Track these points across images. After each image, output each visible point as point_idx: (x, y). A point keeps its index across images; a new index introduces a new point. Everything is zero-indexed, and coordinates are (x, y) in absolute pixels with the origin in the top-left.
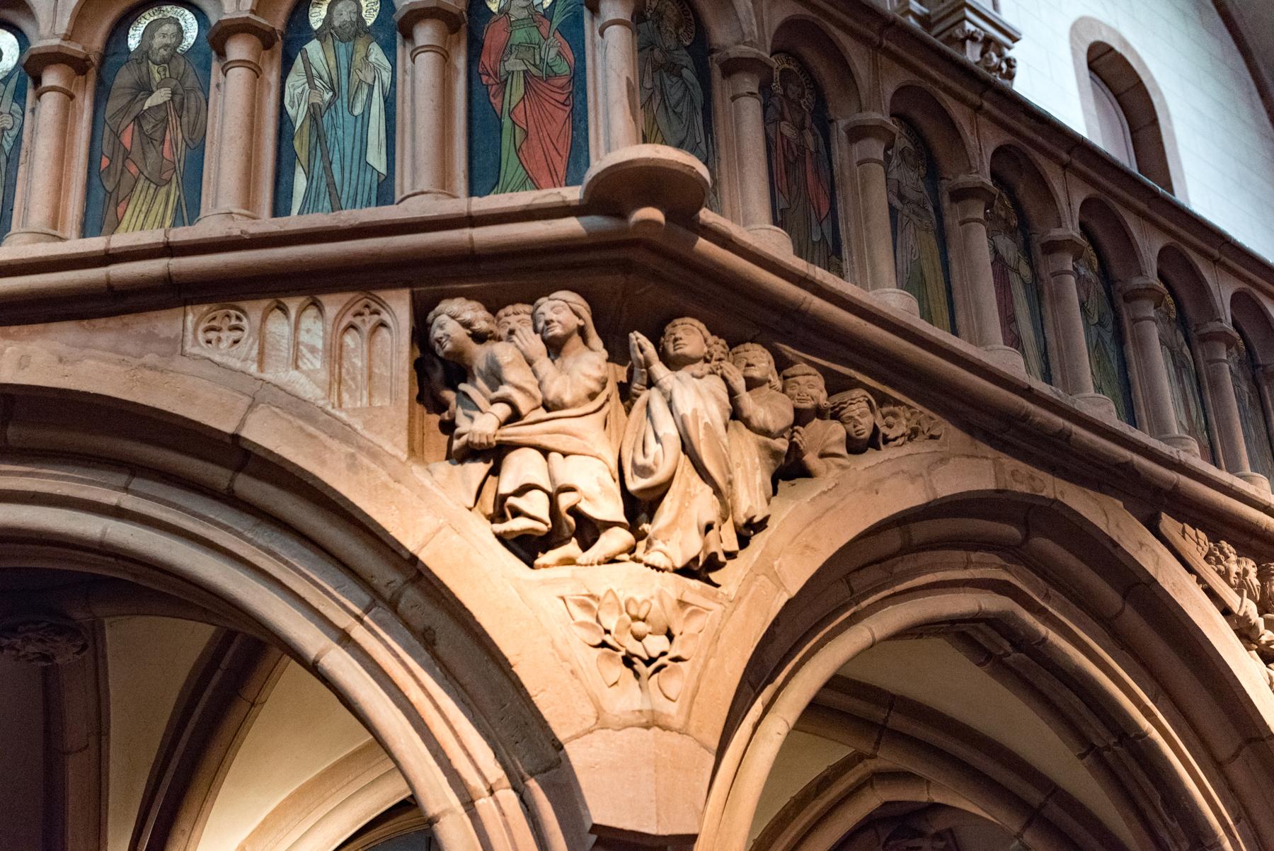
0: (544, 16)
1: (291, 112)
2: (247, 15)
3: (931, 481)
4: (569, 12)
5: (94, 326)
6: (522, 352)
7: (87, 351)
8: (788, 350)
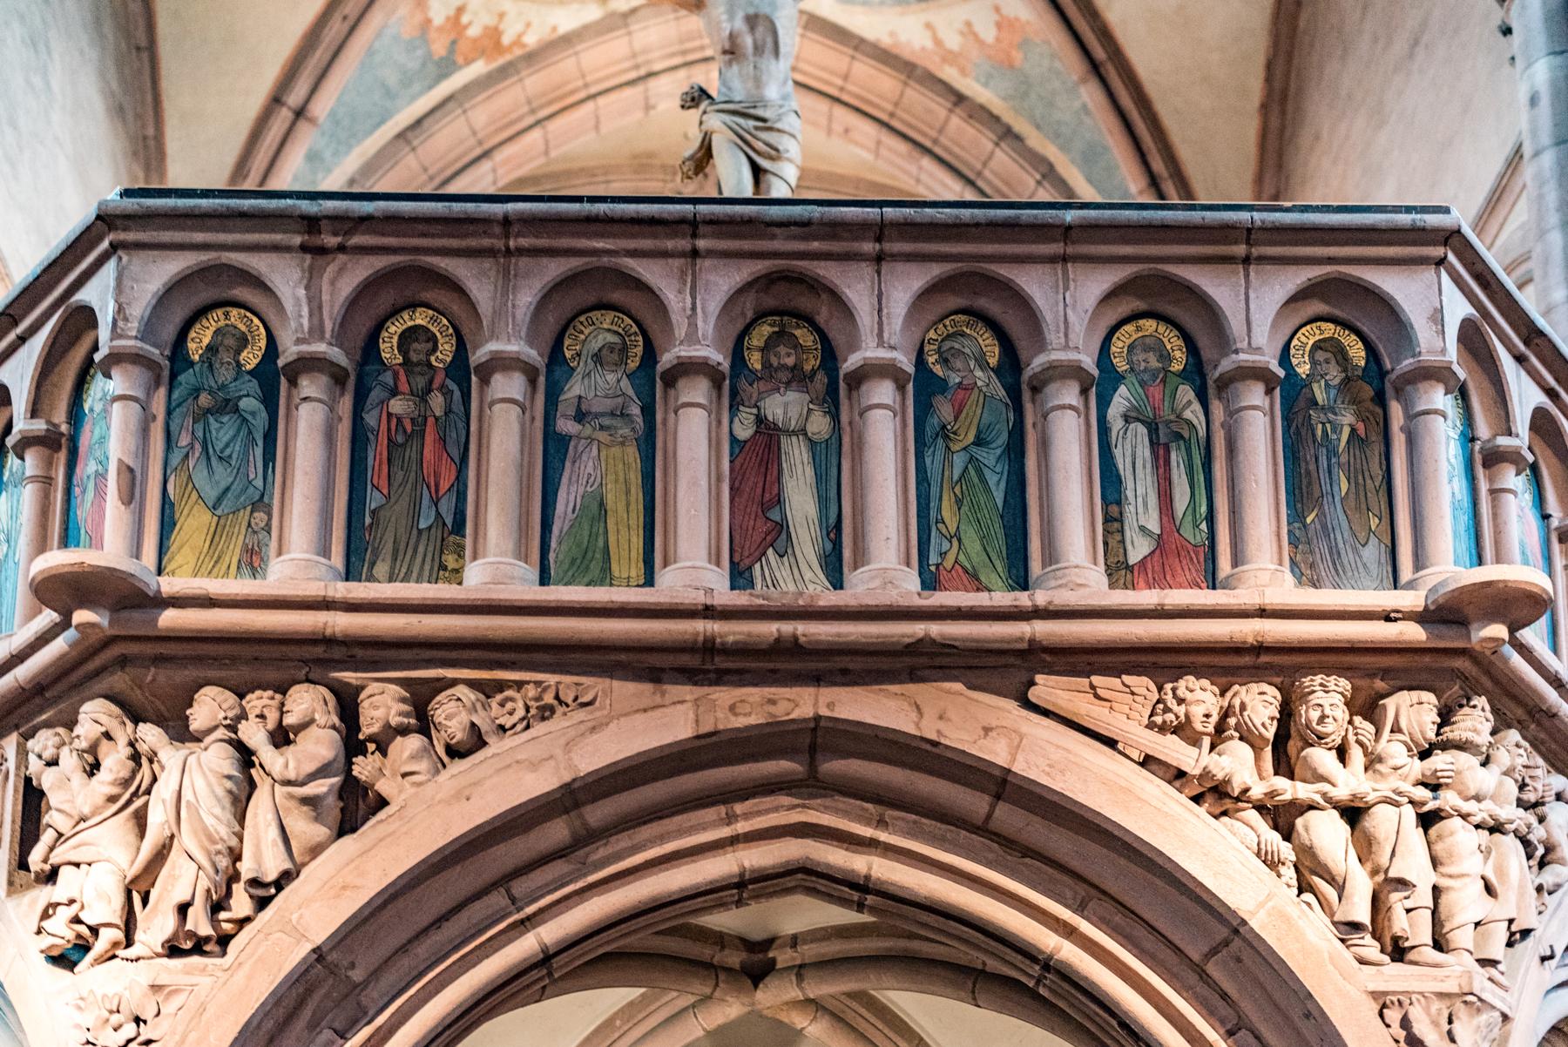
3: (570, 759)
8: (349, 676)
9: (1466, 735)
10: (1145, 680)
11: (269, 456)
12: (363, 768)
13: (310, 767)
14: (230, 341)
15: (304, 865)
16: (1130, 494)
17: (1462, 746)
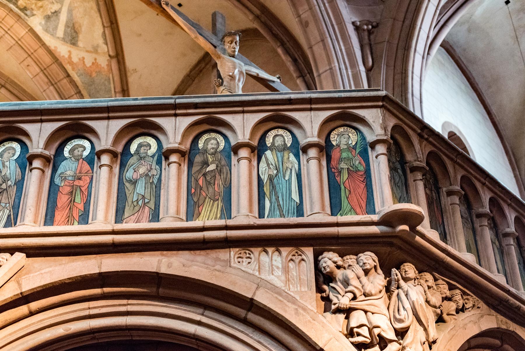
0: (353, 148)
1: (262, 177)
2: (248, 141)
4: (362, 147)
5: (196, 253)
6: (356, 274)
7: (193, 263)
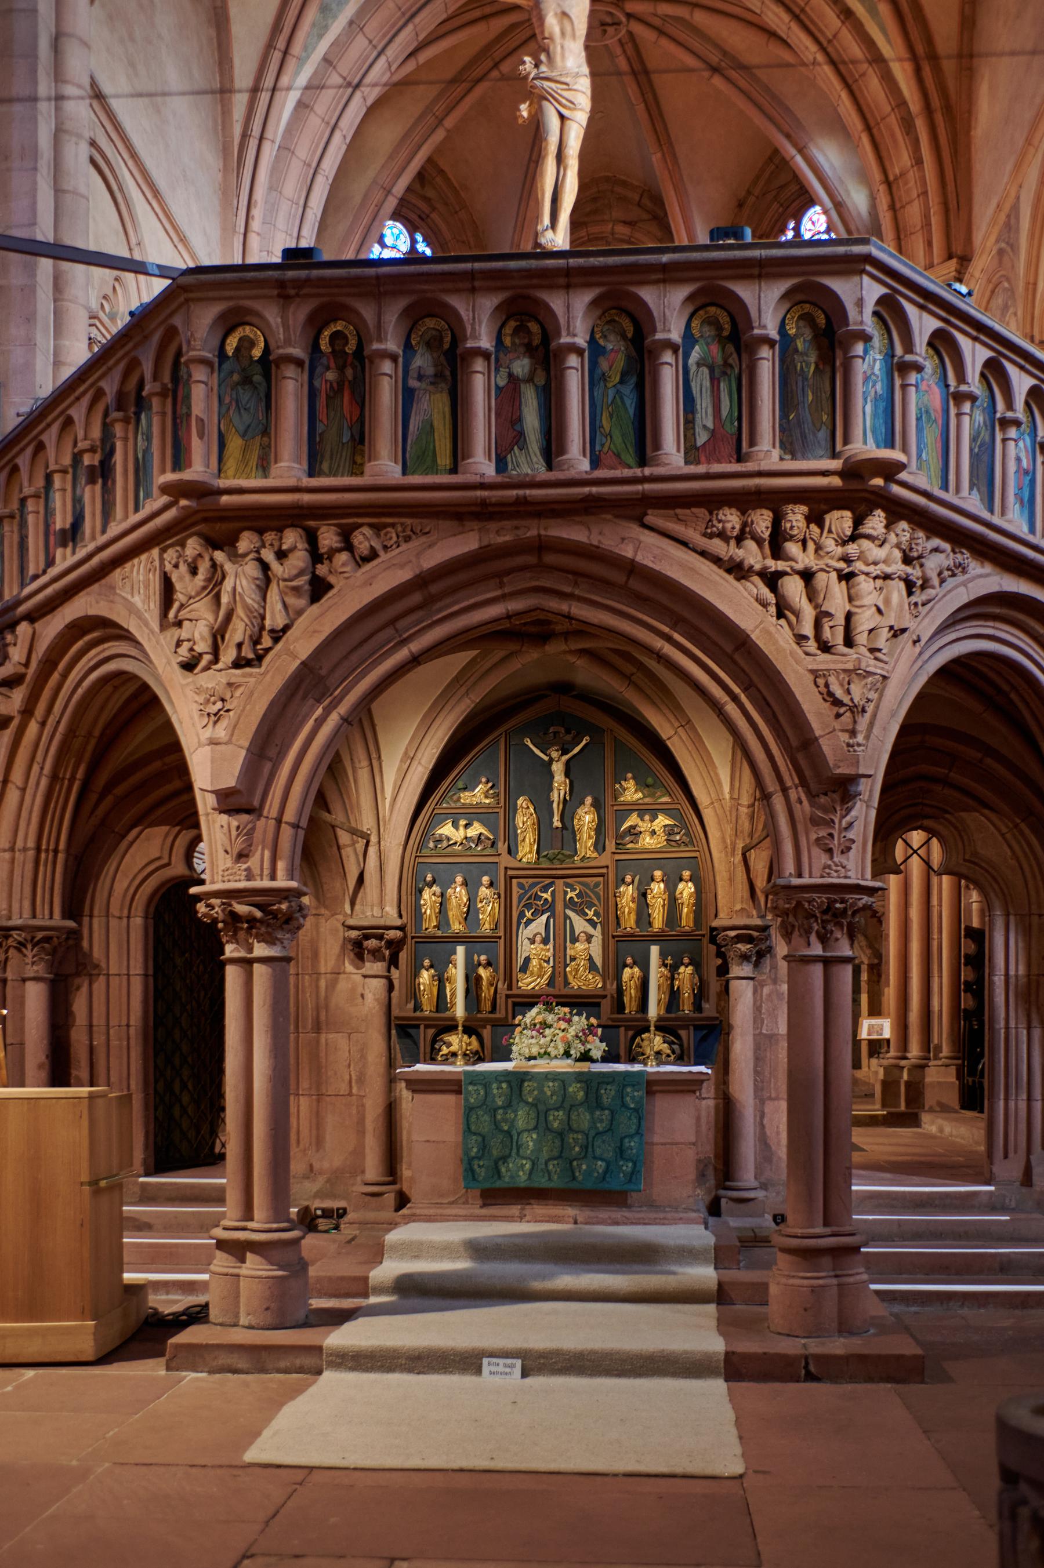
8: (312, 523)
9: (870, 531)
10: (703, 510)
11: (268, 407)
12: (322, 570)
13: (294, 572)
14: (246, 344)
15: (295, 619)
16: (698, 407)
17: (868, 537)
